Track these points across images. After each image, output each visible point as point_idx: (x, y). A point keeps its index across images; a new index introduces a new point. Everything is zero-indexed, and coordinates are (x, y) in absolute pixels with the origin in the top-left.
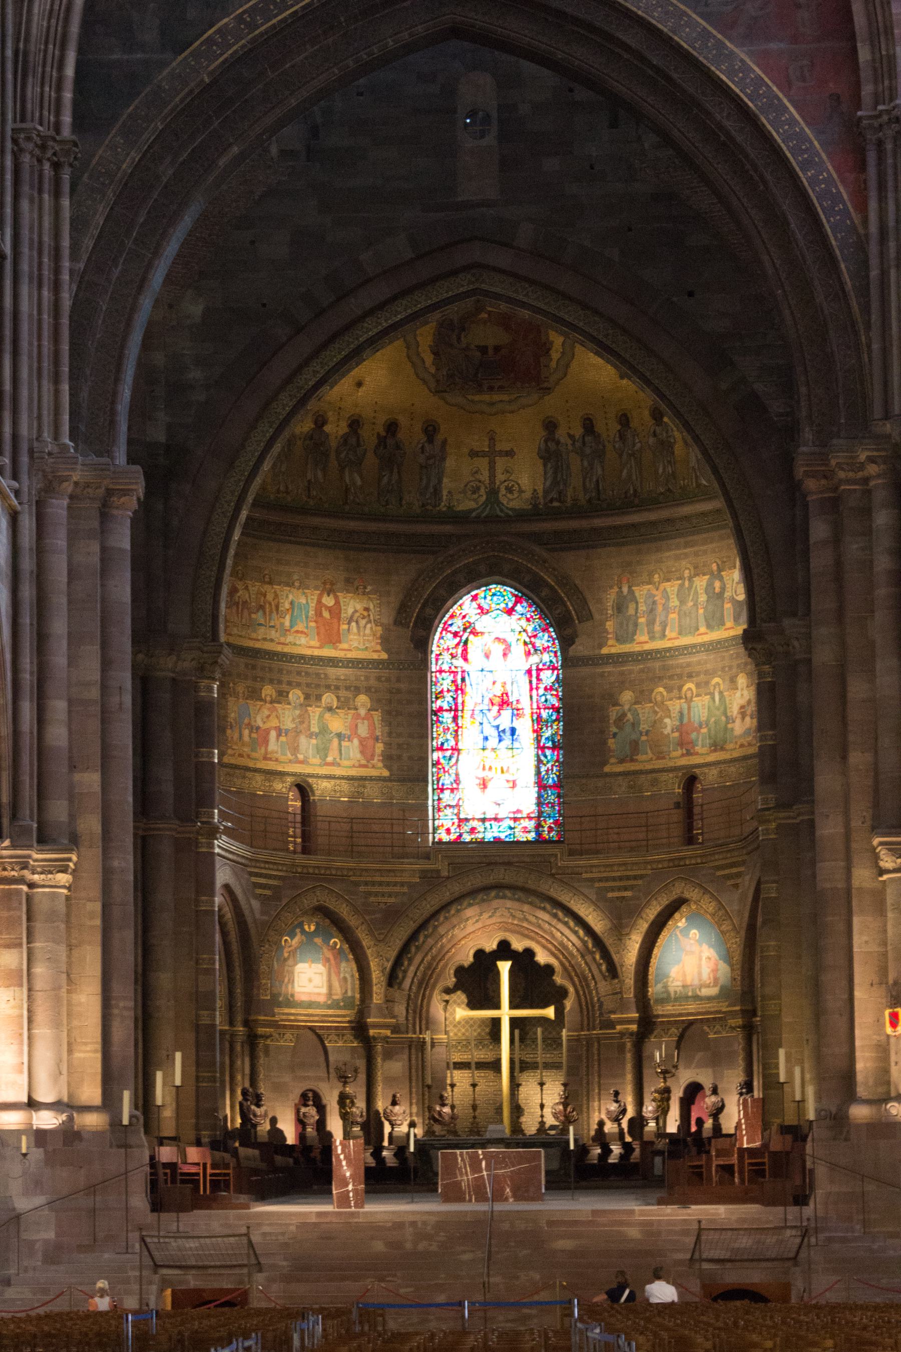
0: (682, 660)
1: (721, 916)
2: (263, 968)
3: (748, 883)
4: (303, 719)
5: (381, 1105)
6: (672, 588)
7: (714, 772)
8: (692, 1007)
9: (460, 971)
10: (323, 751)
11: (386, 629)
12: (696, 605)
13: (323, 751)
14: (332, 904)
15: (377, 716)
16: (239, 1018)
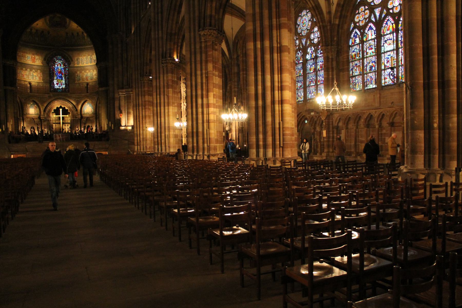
0: (86, 68)
1: (92, 103)
2: (25, 109)
3: (96, 98)
4: (30, 73)
5: (43, 129)
6: (85, 57)
7: (91, 83)
8: (88, 115)
9: (54, 110)
10: (33, 78)
11: (42, 61)
12: (88, 60)
13: (33, 78)
14: (35, 100)
15: (41, 73)
16: (21, 116)
